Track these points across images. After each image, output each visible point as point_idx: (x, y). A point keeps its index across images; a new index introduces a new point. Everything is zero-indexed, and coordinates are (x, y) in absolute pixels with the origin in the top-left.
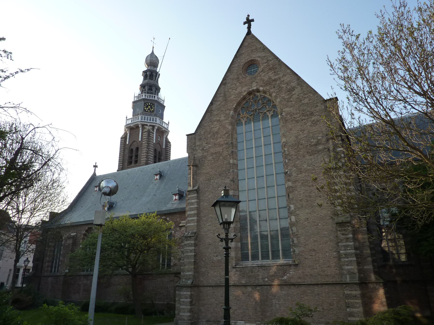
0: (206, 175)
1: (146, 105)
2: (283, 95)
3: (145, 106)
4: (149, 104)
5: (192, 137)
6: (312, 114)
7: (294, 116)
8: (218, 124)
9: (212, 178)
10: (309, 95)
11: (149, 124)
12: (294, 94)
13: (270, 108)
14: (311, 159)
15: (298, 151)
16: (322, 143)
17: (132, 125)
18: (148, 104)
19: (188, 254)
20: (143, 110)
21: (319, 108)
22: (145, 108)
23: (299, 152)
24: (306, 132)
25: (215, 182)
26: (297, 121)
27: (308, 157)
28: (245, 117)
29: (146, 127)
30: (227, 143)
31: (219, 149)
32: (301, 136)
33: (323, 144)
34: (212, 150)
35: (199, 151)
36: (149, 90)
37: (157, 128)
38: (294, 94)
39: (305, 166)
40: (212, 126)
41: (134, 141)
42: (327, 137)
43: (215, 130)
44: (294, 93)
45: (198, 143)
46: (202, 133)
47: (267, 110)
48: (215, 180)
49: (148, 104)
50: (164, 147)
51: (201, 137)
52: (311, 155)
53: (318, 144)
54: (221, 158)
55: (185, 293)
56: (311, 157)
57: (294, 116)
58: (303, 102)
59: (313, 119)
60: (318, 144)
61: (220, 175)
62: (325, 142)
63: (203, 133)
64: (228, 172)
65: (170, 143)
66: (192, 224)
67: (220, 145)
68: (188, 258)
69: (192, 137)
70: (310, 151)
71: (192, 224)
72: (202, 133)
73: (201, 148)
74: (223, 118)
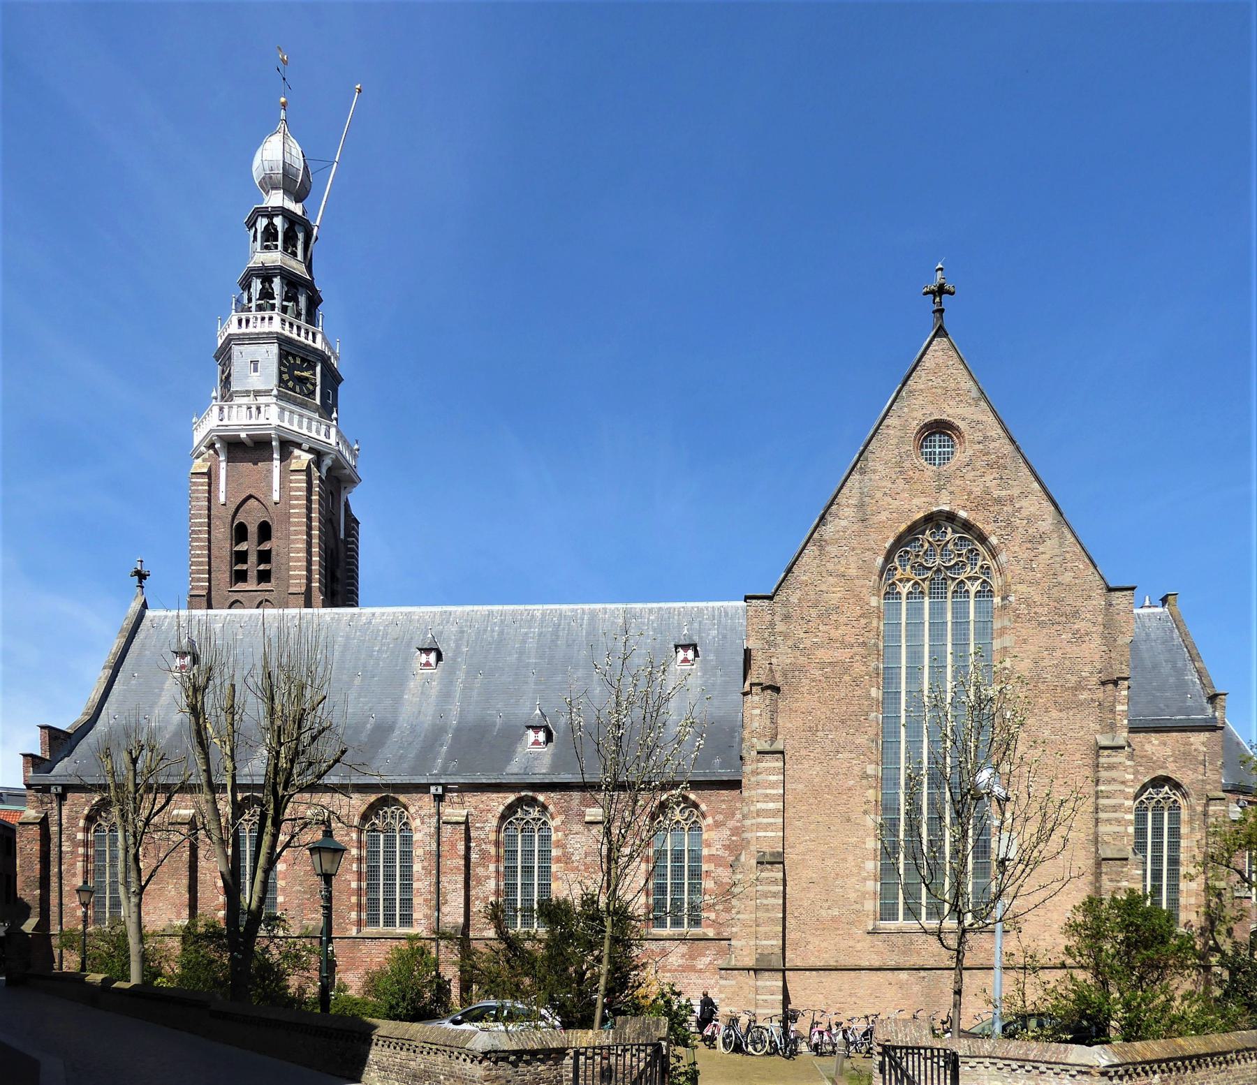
0: (803, 716)
1: (289, 362)
2: (1016, 549)
3: (285, 366)
4: (298, 362)
5: (763, 604)
6: (1076, 614)
7: (1036, 609)
8: (841, 584)
9: (820, 727)
10: (1077, 564)
11: (305, 446)
12: (1042, 553)
13: (976, 573)
14: (1061, 719)
15: (1036, 697)
16: (1089, 687)
17: (243, 435)
18: (292, 362)
19: (765, 902)
20: (275, 381)
21: (1094, 602)
22: (285, 373)
23: (1037, 699)
24: (1058, 653)
25: (830, 736)
26: (1041, 624)
27: (1054, 714)
28: (908, 580)
29: (297, 452)
30: (864, 644)
31: (842, 655)
32: (1046, 663)
33: (1090, 690)
34: (821, 654)
35: (783, 649)
36: (287, 299)
37: (327, 462)
38: (1042, 553)
39: (1047, 733)
40: (824, 588)
41: (250, 497)
42: (1100, 675)
43: (834, 598)
44: (1041, 549)
45: (780, 627)
46: (794, 599)
47: (966, 575)
48: (827, 733)
49: (292, 362)
50: (342, 536)
51: (791, 610)
52: (1061, 711)
53: (1079, 687)
54: (847, 678)
55: (768, 983)
56: (1061, 715)
57: (1036, 609)
58: (1060, 579)
59: (1076, 626)
60: (1079, 687)
61: (843, 722)
62: (1095, 687)
63: (796, 601)
64: (863, 717)
65: (357, 523)
66: (773, 834)
67: (844, 645)
68: (767, 910)
69: (763, 604)
70: (1061, 700)
71: (773, 834)
72: (794, 599)
73: (790, 643)
74: (853, 572)
